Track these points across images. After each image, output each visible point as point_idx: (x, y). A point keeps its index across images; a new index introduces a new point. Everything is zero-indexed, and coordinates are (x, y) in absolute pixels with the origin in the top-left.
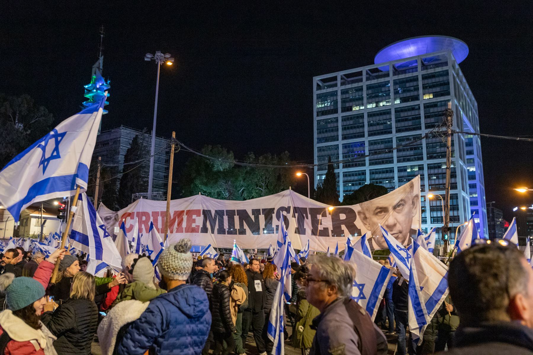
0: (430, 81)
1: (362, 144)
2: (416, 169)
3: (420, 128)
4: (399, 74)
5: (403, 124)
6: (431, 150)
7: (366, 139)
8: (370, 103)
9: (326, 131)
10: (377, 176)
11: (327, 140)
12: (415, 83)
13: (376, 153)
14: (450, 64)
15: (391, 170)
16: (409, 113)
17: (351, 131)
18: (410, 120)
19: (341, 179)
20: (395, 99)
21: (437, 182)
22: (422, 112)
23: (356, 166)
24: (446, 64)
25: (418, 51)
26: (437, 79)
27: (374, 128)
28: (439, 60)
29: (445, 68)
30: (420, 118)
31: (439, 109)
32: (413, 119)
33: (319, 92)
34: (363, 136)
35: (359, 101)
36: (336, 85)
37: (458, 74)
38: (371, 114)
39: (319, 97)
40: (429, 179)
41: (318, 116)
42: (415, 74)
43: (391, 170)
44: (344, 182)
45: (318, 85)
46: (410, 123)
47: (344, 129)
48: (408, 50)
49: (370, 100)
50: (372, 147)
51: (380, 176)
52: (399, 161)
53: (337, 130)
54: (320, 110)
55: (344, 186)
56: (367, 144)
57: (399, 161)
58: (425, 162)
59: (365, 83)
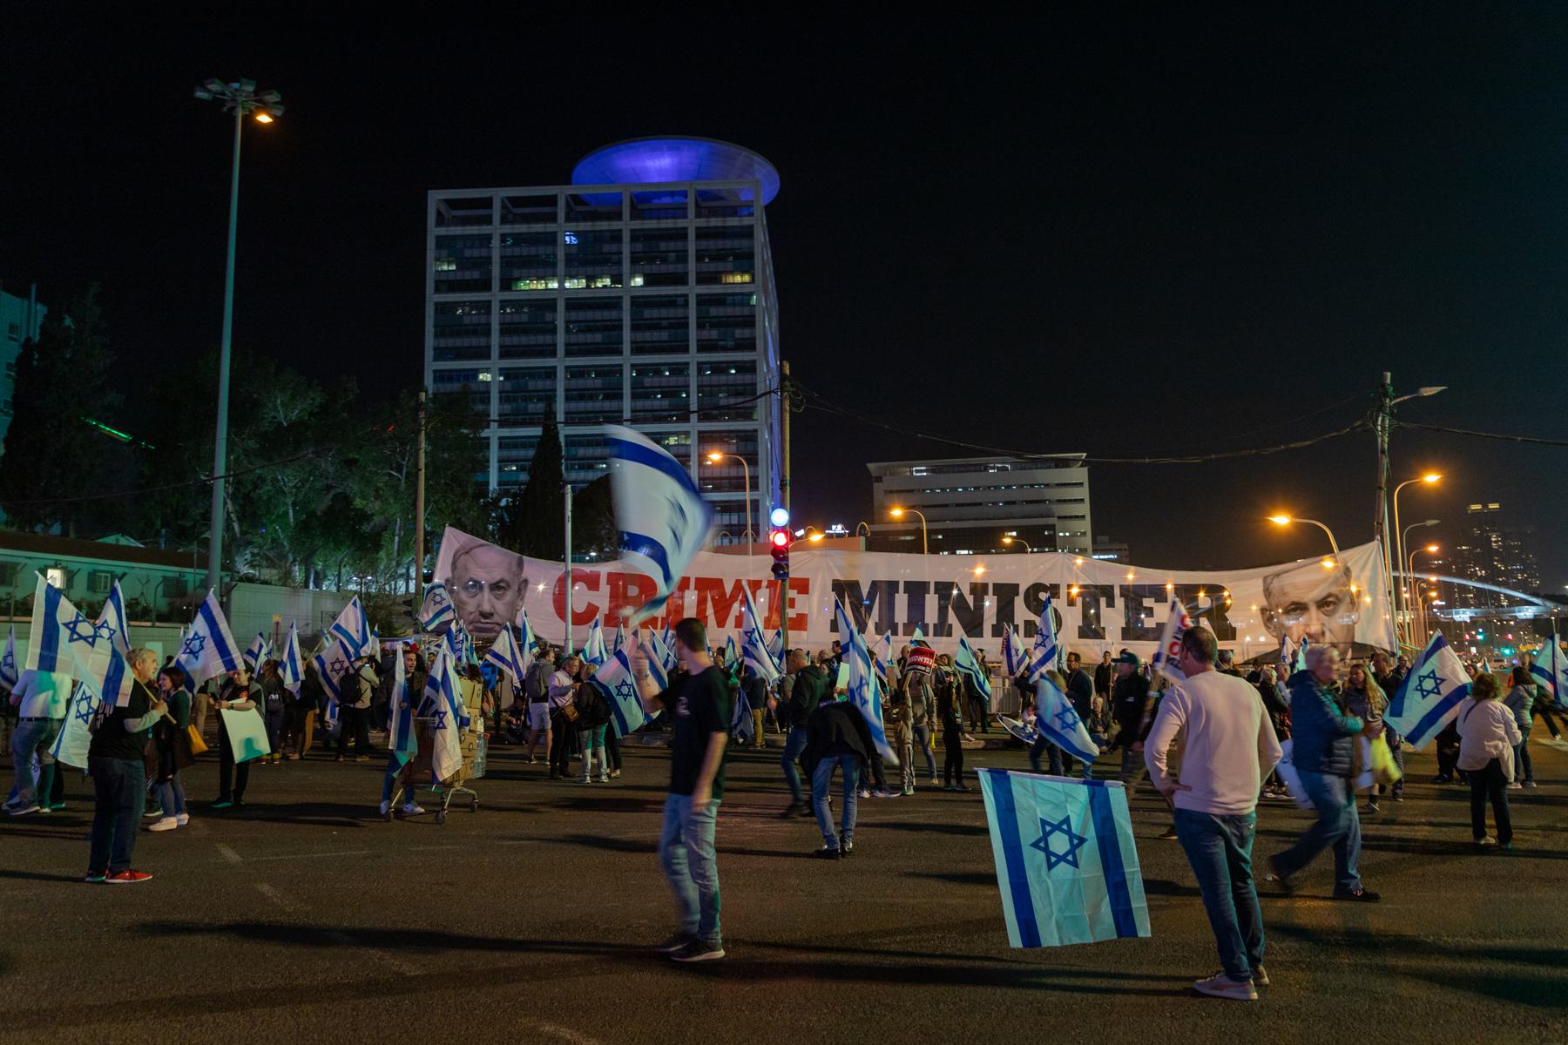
0: (711, 244)
1: (551, 373)
3: (686, 350)
7: (560, 362)
8: (572, 277)
9: (459, 334)
11: (459, 354)
12: (680, 245)
13: (581, 398)
16: (664, 312)
17: (524, 340)
19: (494, 454)
20: (633, 275)
26: (728, 244)
27: (581, 338)
28: (722, 198)
29: (747, 221)
31: (729, 311)
32: (670, 327)
33: (442, 231)
34: (554, 354)
35: (545, 268)
36: (488, 220)
38: (576, 303)
39: (441, 242)
41: (437, 290)
42: (681, 223)
44: (500, 461)
45: (439, 214)
46: (664, 335)
47: (506, 330)
48: (659, 163)
49: (574, 271)
50: (574, 383)
51: (590, 451)
53: (488, 333)
54: (443, 278)
55: (500, 470)
56: (561, 374)
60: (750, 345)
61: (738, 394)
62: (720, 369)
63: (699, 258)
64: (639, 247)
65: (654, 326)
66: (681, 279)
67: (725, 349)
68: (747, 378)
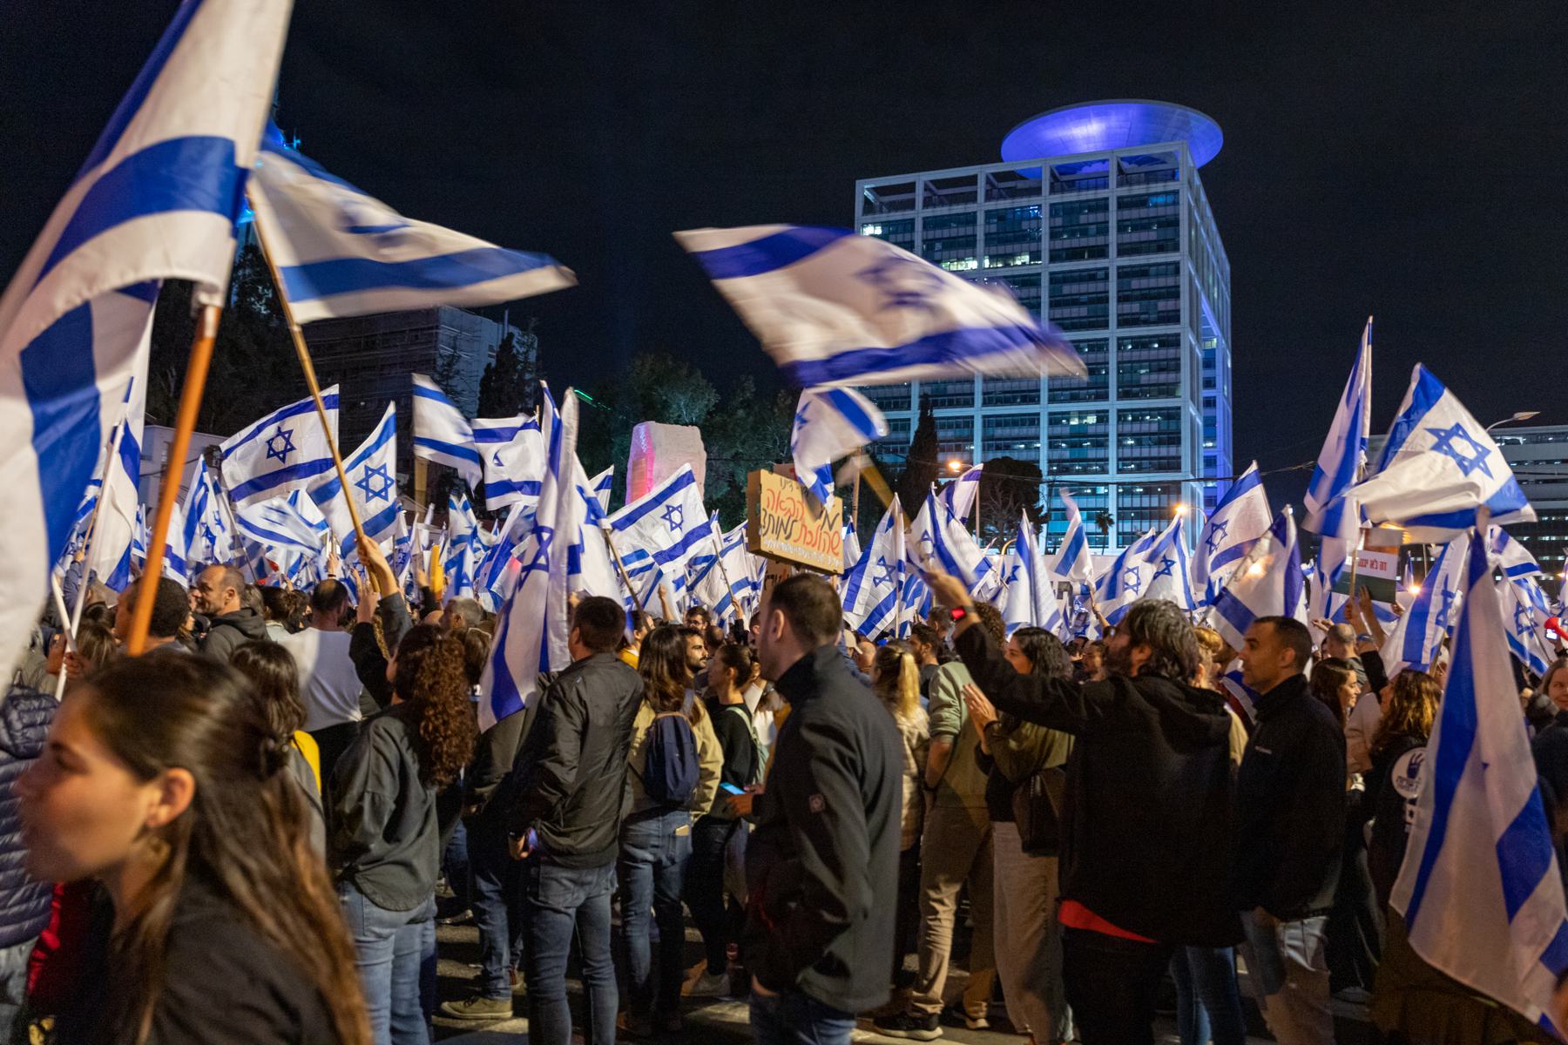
0: (1135, 213)
2: (1092, 419)
3: (1106, 325)
4: (1063, 191)
5: (1066, 312)
6: (1127, 377)
10: (999, 432)
12: (1100, 217)
14: (1183, 175)
15: (1033, 420)
16: (1083, 287)
18: (1084, 304)
21: (1136, 453)
22: (1113, 288)
23: (951, 404)
24: (1173, 175)
25: (1109, 136)
29: (1171, 186)
30: (1106, 300)
31: (1153, 282)
32: (1090, 302)
37: (1197, 200)
40: (1120, 444)
42: (1101, 194)
43: (1033, 420)
46: (1083, 311)
48: (1086, 132)
51: (1007, 432)
52: (1052, 400)
57: (1052, 400)
58: (1113, 405)
59: (981, 206)
60: (1174, 317)
61: (1161, 370)
62: (1141, 343)
63: (1121, 228)
64: (1059, 221)
65: (1074, 302)
66: (1101, 252)
67: (1147, 323)
68: (1171, 352)
